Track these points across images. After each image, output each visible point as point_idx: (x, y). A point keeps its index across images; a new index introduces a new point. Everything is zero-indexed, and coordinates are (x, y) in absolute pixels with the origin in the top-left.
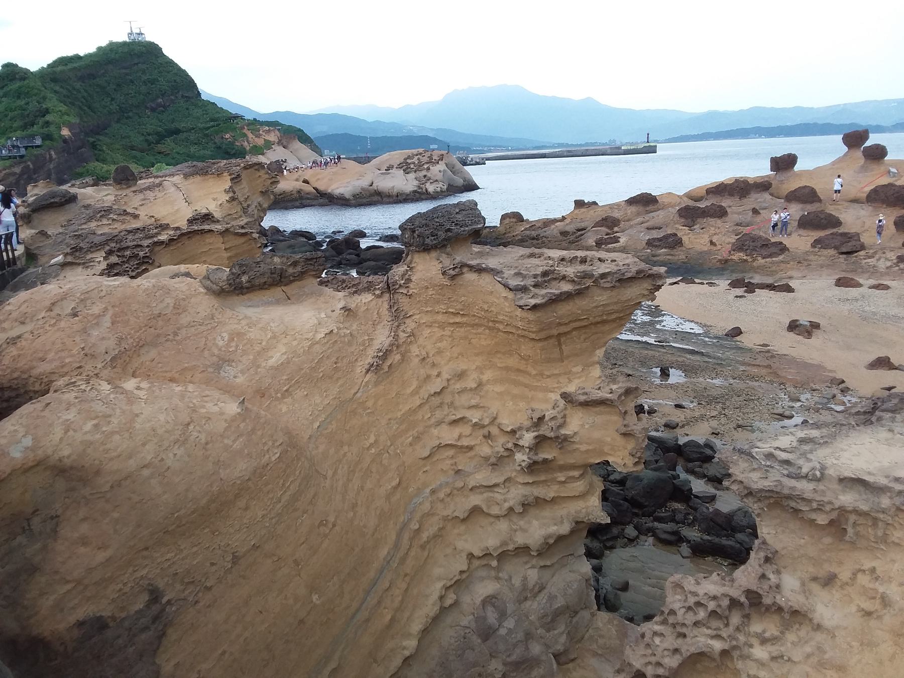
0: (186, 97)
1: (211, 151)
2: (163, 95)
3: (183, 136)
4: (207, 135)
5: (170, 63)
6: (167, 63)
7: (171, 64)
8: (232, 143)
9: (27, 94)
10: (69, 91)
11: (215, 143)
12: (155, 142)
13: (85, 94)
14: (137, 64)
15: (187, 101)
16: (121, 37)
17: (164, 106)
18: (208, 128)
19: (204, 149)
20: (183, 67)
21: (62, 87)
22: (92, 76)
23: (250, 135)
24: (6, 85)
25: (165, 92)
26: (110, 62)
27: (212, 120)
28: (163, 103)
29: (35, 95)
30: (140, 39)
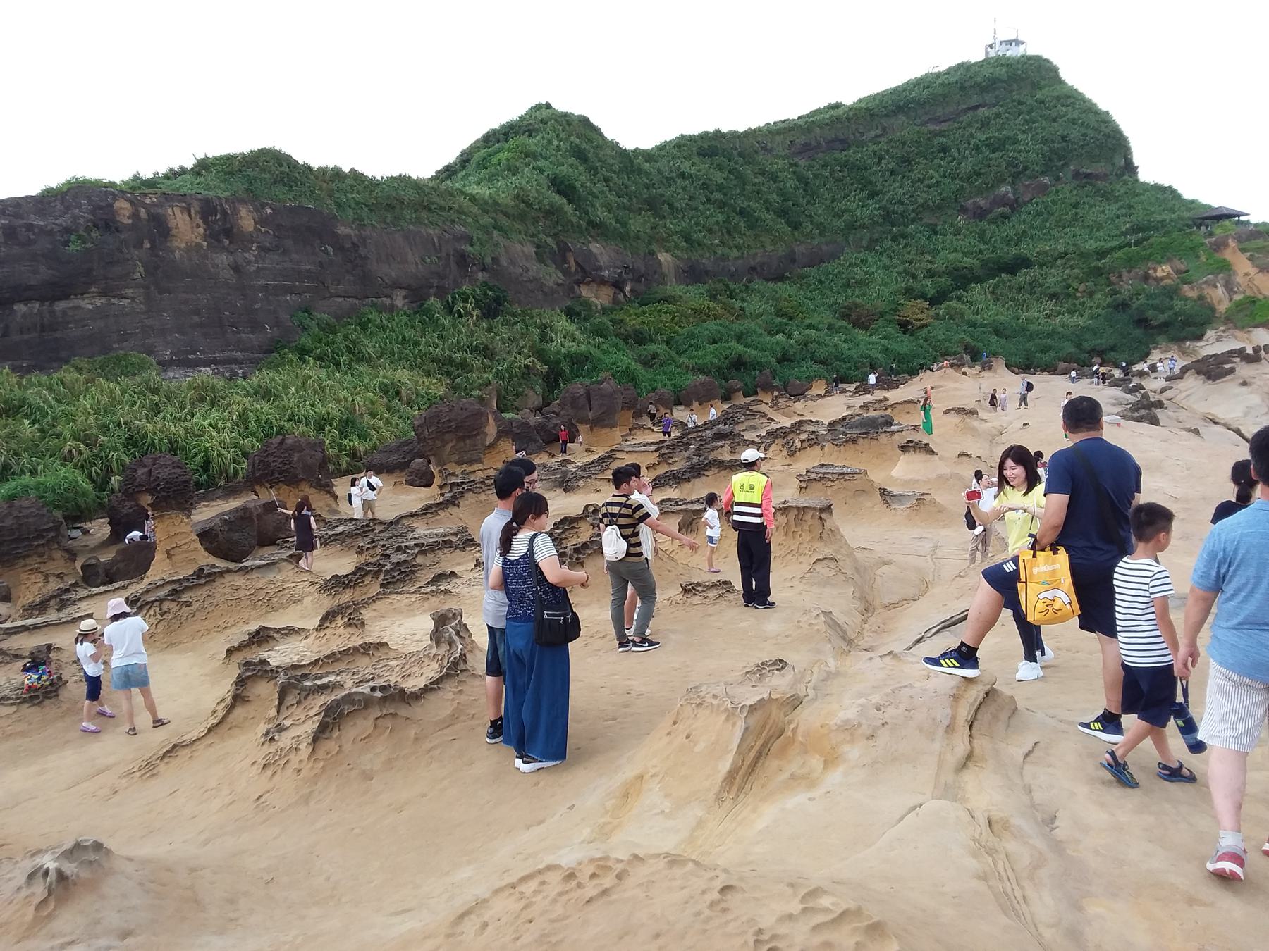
0: (1087, 176)
3: (1022, 277)
4: (1098, 272)
6: (1058, 98)
7: (1073, 99)
8: (1172, 292)
13: (790, 184)
14: (976, 107)
17: (1015, 205)
18: (1101, 254)
19: (1071, 312)
20: (1103, 106)
21: (720, 167)
22: (844, 144)
23: (1242, 265)
25: (1026, 168)
27: (1137, 229)
28: (1011, 195)
30: (1008, 54)
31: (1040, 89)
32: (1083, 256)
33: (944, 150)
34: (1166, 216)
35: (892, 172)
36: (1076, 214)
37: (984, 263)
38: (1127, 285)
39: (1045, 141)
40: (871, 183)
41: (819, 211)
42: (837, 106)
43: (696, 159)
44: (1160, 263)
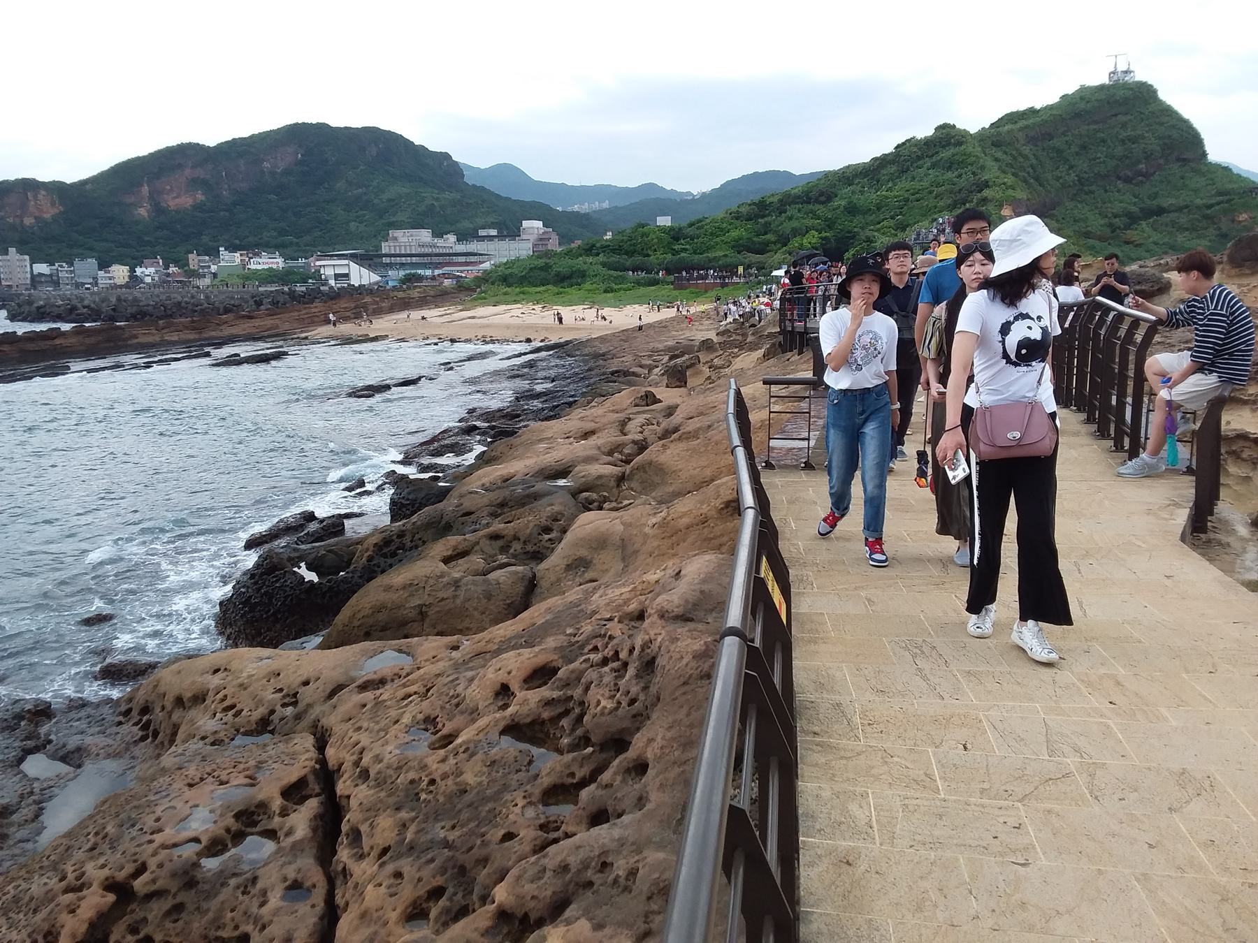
0: (1184, 160)
1: (1210, 241)
2: (1146, 158)
3: (1166, 218)
4: (1206, 217)
5: (1167, 110)
7: (1168, 112)
9: (962, 164)
10: (1015, 158)
11: (1219, 229)
12: (1122, 226)
13: (1034, 161)
15: (1184, 166)
16: (1099, 78)
17: (1147, 175)
18: (1210, 207)
19: (1198, 238)
21: (1006, 153)
24: (937, 153)
25: (1152, 154)
26: (1077, 115)
27: (1220, 194)
28: (1144, 170)
29: (972, 165)
30: (1126, 79)
31: (1150, 104)
32: (1198, 208)
33: (1104, 141)
34: (1235, 186)
35: (1077, 154)
36: (1184, 183)
37: (1142, 210)
38: (1225, 225)
39: (1159, 138)
40: (1068, 160)
41: (1049, 176)
42: (1032, 112)
43: (994, 148)
44: (1241, 213)
